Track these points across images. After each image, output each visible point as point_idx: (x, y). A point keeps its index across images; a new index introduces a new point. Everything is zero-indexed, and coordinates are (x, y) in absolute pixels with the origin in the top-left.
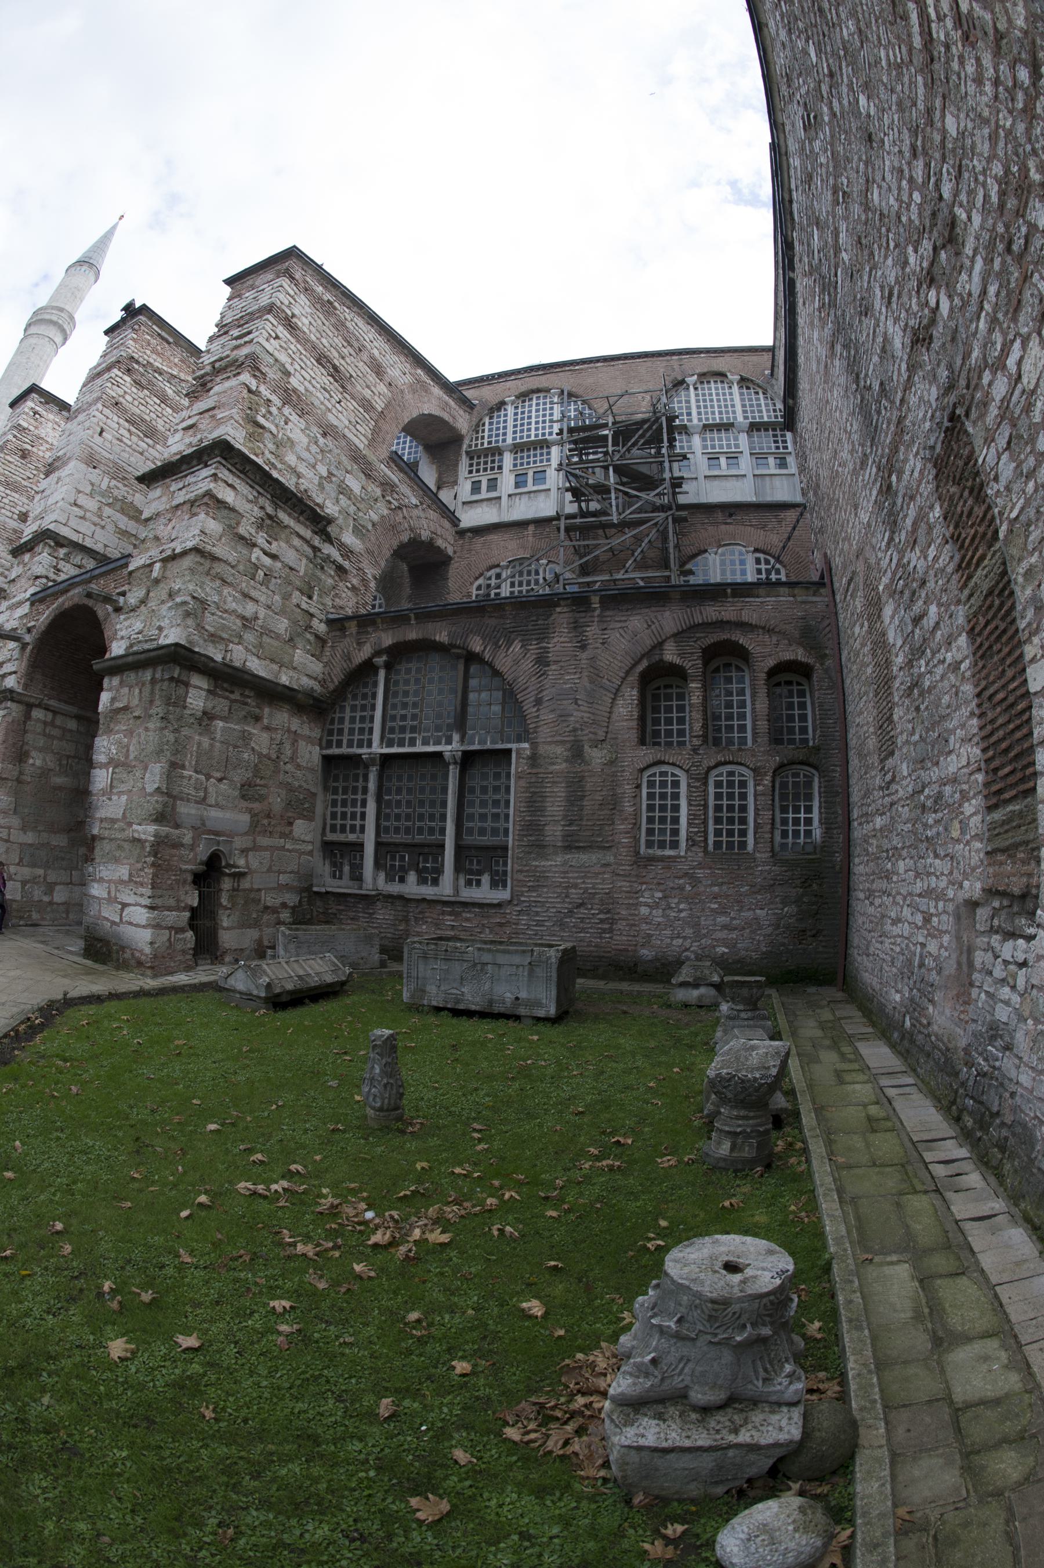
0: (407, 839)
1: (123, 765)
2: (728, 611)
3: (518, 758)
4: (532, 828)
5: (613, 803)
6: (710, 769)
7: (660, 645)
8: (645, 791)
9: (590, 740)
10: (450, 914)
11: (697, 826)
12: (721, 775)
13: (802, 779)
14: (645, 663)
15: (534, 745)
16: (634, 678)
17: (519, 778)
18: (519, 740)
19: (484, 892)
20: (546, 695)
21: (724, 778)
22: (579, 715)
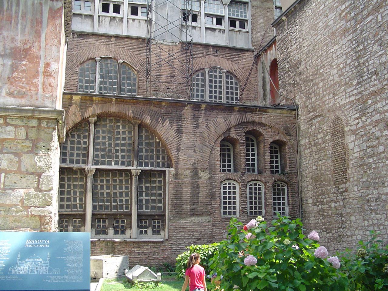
0: (108, 212)
1: (15, 172)
2: (257, 118)
3: (169, 174)
4: (177, 206)
5: (212, 196)
6: (248, 182)
7: (229, 130)
8: (222, 190)
9: (201, 168)
10: (137, 247)
11: (244, 205)
12: (252, 185)
13: (281, 187)
14: (223, 137)
15: (177, 169)
16: (218, 143)
17: (169, 184)
18: (168, 166)
19: (150, 236)
20: (182, 147)
21: (253, 186)
22: (197, 157)
